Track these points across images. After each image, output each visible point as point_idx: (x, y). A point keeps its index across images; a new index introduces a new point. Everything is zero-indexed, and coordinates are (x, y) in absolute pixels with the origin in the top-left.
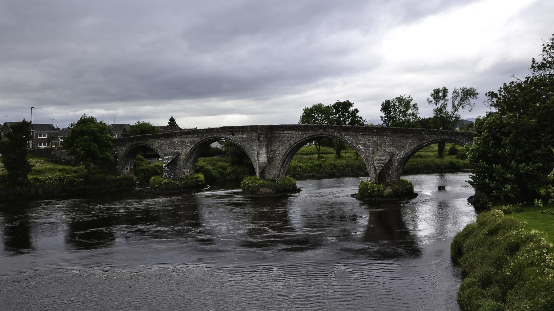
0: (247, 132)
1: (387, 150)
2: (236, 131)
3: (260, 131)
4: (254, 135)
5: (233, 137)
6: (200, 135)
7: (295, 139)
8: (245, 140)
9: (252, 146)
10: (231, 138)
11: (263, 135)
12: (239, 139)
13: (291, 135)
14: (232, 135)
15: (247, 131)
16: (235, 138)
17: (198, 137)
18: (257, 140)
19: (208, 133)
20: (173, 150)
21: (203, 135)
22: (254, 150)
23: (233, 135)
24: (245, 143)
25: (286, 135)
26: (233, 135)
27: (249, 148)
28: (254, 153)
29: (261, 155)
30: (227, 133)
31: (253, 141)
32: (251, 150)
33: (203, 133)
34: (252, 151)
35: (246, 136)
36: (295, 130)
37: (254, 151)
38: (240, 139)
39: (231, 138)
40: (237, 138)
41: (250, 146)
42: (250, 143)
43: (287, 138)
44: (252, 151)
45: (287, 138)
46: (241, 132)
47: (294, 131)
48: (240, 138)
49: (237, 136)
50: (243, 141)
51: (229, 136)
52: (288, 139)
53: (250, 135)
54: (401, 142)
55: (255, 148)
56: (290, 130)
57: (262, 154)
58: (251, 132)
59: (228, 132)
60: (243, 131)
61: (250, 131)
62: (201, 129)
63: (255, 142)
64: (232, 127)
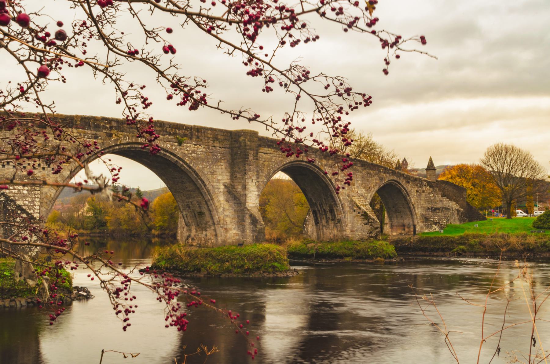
0: (206, 141)
1: (359, 192)
2: (185, 135)
3: (248, 141)
4: (218, 148)
5: (178, 147)
6: (102, 133)
7: (274, 165)
8: (201, 158)
9: (214, 171)
10: (176, 149)
11: (253, 150)
12: (191, 154)
13: (269, 157)
14: (176, 144)
15: (206, 138)
16: (182, 151)
17: (96, 137)
18: (223, 161)
19: (123, 131)
20: (14, 166)
21: (110, 135)
22: (218, 181)
23: (180, 144)
24: (202, 165)
25: (263, 156)
26: (180, 144)
27: (210, 177)
28: (219, 189)
29: (251, 191)
30: (166, 136)
31: (217, 161)
32: (213, 182)
33: (111, 128)
34: (215, 184)
35: (204, 150)
36: (273, 148)
37: (217, 184)
38: (193, 155)
39: (176, 149)
40: (186, 152)
41: (211, 172)
42: (212, 166)
43: (265, 161)
44: (215, 184)
45: (265, 161)
46: (194, 140)
47: (273, 150)
48: (194, 152)
49: (187, 147)
50: (198, 159)
51: (172, 146)
52: (266, 163)
53: (212, 149)
54: (368, 180)
55: (220, 177)
56: (269, 146)
57: (251, 189)
58: (214, 141)
59: (170, 134)
60: (198, 137)
61: (211, 139)
62: (104, 119)
63: (219, 164)
64: (177, 124)
